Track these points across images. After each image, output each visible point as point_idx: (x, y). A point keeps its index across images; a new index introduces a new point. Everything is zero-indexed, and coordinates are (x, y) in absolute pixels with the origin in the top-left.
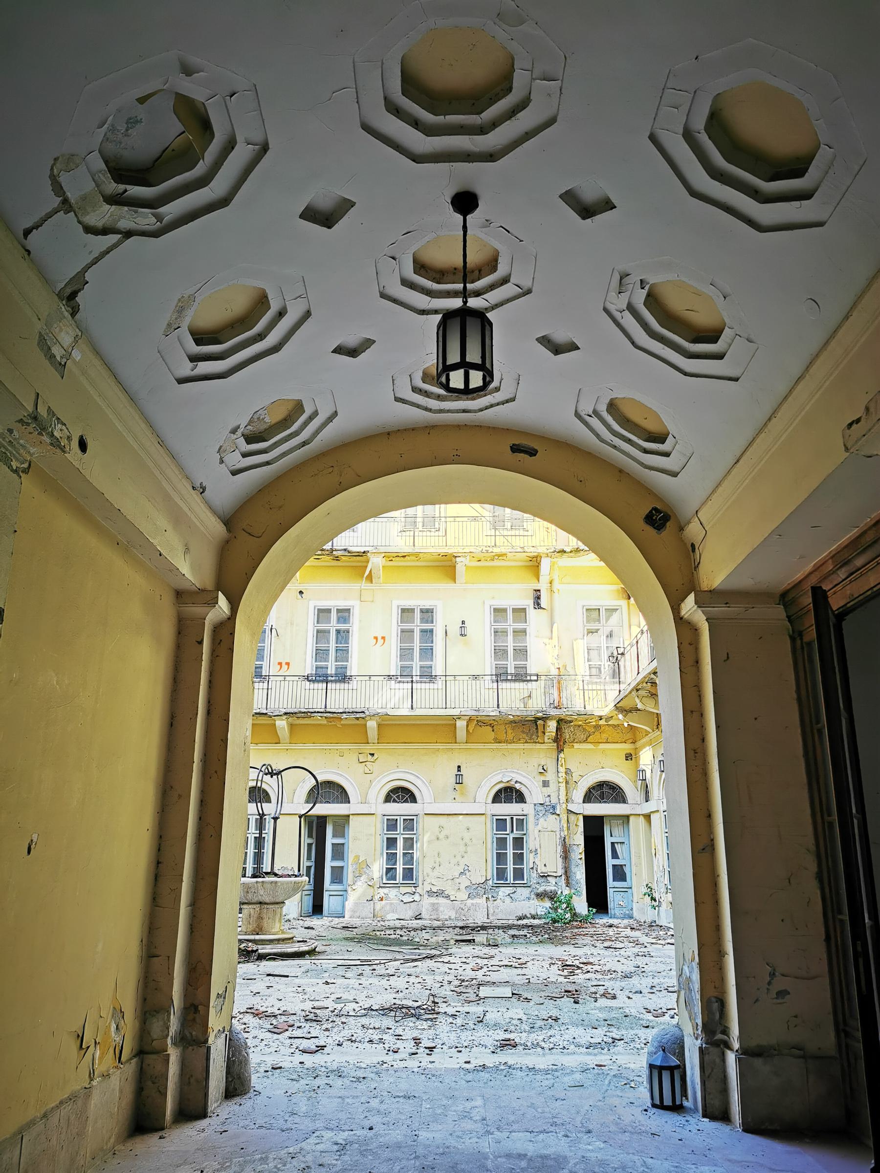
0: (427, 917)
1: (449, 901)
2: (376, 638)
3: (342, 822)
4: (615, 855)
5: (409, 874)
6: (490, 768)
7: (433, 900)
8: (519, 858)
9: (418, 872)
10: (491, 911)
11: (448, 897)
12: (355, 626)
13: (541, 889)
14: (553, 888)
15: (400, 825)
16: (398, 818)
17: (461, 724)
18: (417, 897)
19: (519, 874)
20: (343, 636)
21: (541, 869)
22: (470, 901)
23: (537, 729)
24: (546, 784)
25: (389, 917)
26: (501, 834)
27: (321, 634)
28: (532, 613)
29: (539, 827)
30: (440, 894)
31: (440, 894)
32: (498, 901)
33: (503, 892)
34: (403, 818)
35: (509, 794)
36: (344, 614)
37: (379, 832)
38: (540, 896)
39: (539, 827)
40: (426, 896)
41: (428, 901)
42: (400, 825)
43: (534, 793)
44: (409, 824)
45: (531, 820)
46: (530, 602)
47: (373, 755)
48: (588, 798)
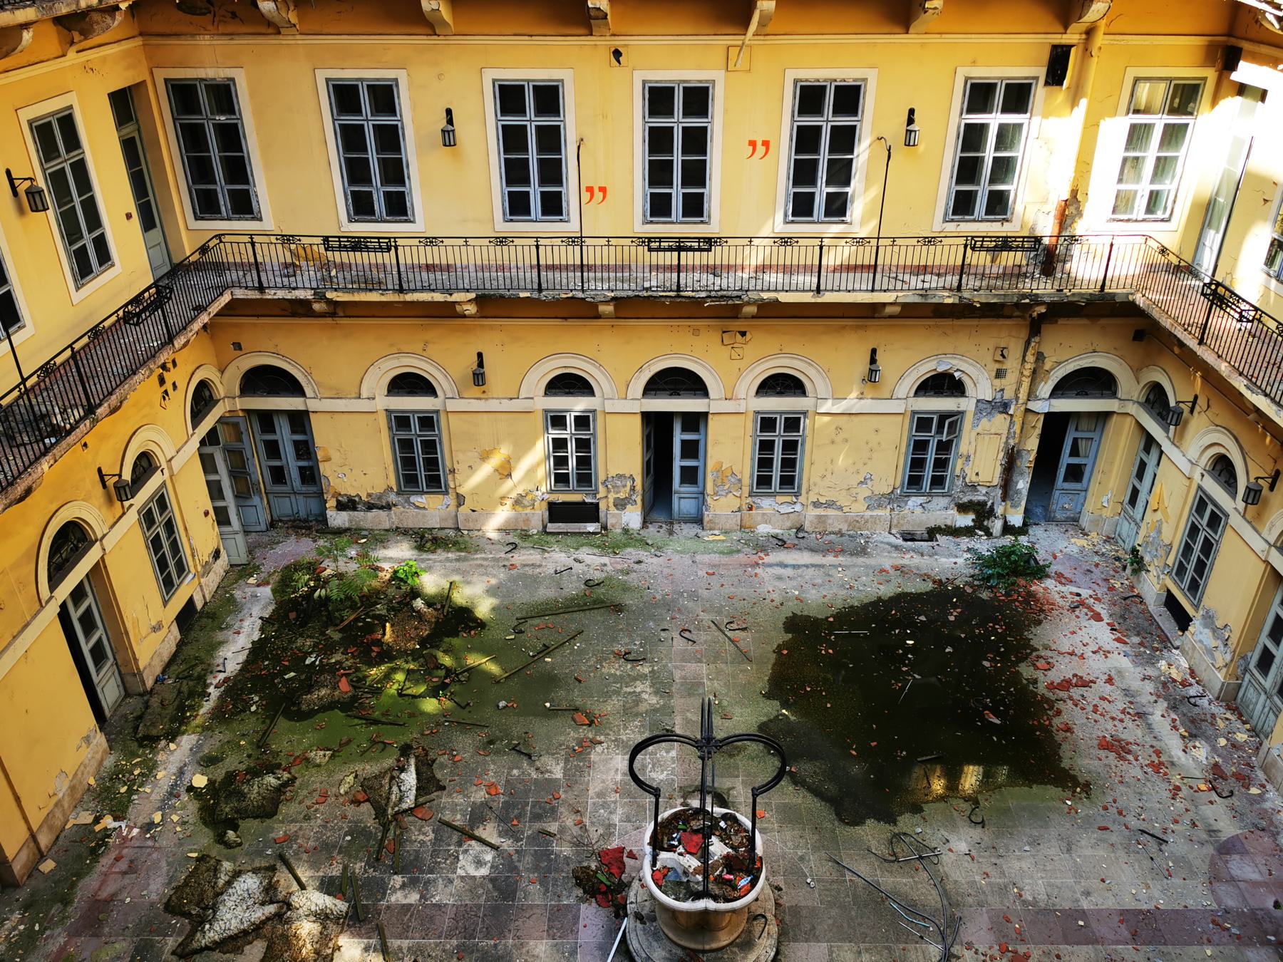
0: (810, 530)
2: (753, 144)
3: (695, 421)
4: (1075, 452)
7: (820, 512)
8: (941, 464)
9: (801, 479)
10: (895, 522)
11: (841, 508)
12: (719, 124)
13: (965, 500)
14: (982, 498)
18: (798, 508)
19: (938, 481)
20: (697, 141)
21: (971, 478)
22: (869, 513)
24: (1000, 374)
26: (922, 436)
29: (979, 429)
31: (830, 504)
33: (914, 502)
36: (698, 99)
37: (750, 431)
38: (963, 508)
39: (979, 429)
40: (811, 507)
41: (813, 512)
42: (780, 425)
43: (981, 386)
44: (793, 423)
46: (1042, 72)
48: (1061, 389)
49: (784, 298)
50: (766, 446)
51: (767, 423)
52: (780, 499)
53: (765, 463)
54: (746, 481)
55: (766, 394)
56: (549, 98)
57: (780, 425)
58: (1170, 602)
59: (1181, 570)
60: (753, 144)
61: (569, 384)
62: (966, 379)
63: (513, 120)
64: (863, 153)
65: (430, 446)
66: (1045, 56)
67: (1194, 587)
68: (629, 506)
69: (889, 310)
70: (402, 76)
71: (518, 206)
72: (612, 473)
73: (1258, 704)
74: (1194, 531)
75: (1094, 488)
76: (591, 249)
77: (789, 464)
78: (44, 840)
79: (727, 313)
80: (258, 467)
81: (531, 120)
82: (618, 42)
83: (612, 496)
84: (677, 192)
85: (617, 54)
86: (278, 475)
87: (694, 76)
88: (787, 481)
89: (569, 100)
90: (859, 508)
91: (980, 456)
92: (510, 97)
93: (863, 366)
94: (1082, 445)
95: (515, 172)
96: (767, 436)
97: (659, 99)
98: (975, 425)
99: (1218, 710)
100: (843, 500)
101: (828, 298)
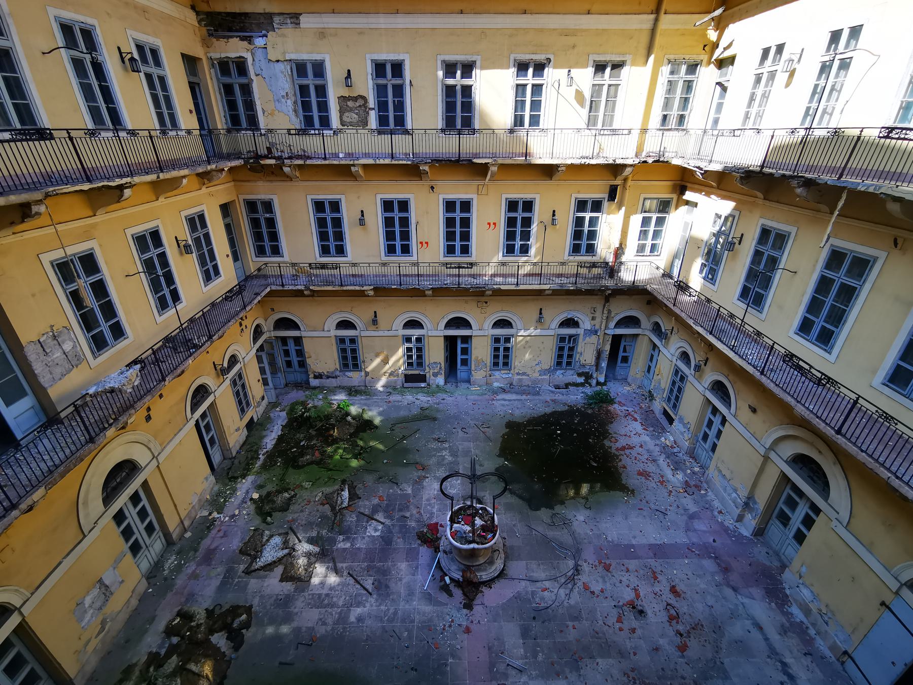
2: (489, 224)
3: (466, 339)
4: (625, 351)
7: (519, 377)
8: (570, 356)
12: (475, 216)
19: (569, 364)
20: (466, 223)
21: (583, 362)
24: (593, 319)
26: (562, 344)
30: (524, 374)
31: (524, 374)
33: (559, 372)
35: (570, 323)
36: (466, 206)
38: (579, 375)
42: (502, 341)
45: (581, 337)
46: (606, 196)
48: (619, 324)
49: (503, 287)
50: (497, 349)
51: (497, 340)
52: (503, 372)
53: (496, 357)
54: (488, 364)
56: (404, 205)
57: (502, 341)
58: (665, 413)
59: (669, 399)
60: (489, 224)
61: (413, 324)
62: (580, 321)
63: (389, 215)
64: (534, 228)
65: (354, 351)
66: (608, 190)
67: (675, 406)
69: (547, 292)
70: (343, 197)
71: (391, 250)
72: (432, 361)
73: (703, 455)
74: (674, 383)
75: (632, 366)
77: (506, 357)
78: (187, 523)
79: (480, 294)
80: (280, 361)
81: (397, 215)
82: (433, 183)
83: (432, 371)
84: (458, 244)
85: (432, 188)
86: (289, 364)
87: (464, 196)
88: (506, 364)
89: (412, 206)
90: (536, 375)
91: (586, 353)
92: (388, 205)
93: (537, 315)
94: (627, 348)
95: (390, 236)
96: (497, 345)
97: (450, 206)
98: (584, 340)
99: (686, 458)
100: (529, 372)
101: (522, 287)
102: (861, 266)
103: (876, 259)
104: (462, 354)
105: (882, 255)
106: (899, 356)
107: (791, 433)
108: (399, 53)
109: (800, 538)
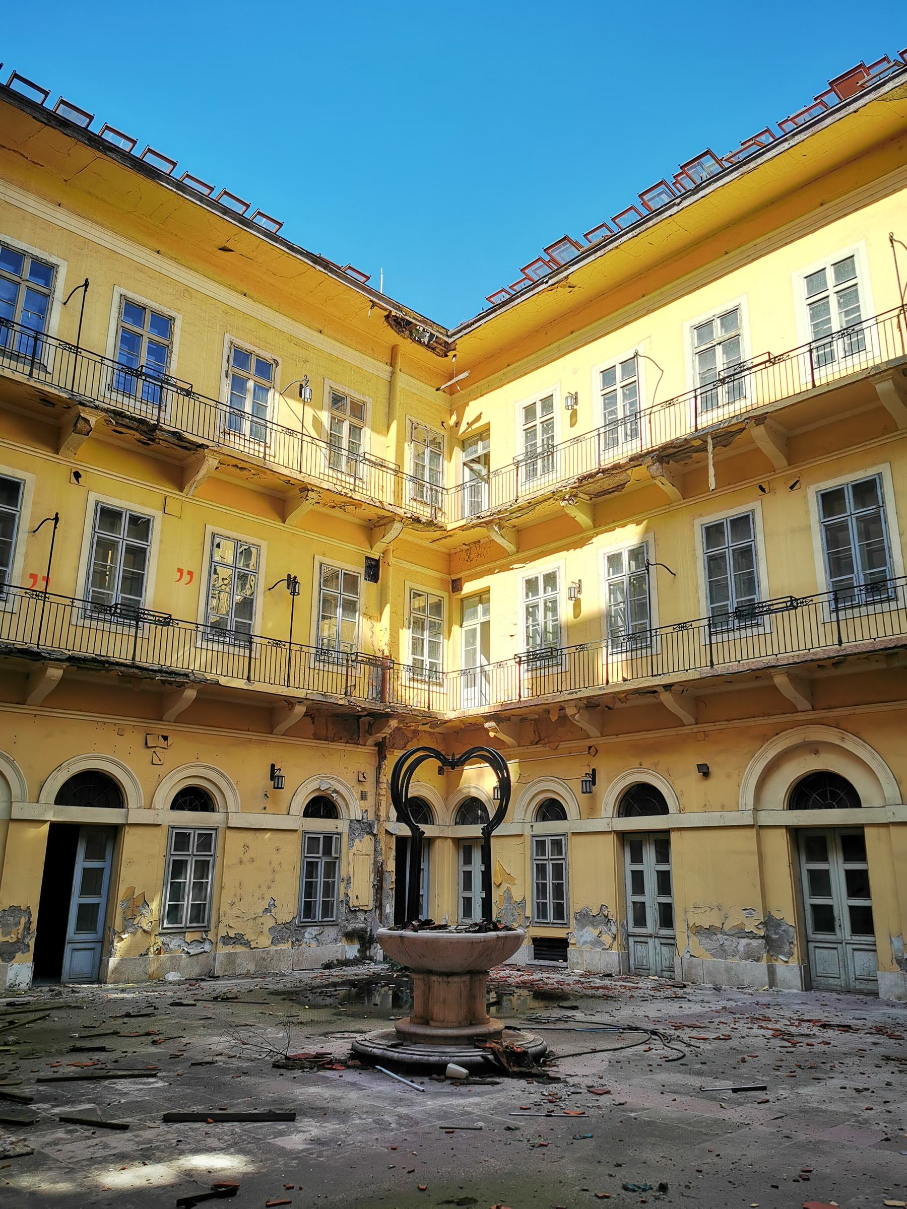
1: (247, 950)
2: (180, 571)
5: (198, 913)
6: (312, 769)
7: (229, 949)
8: (329, 889)
13: (350, 928)
14: (363, 925)
15: (194, 841)
16: (192, 831)
17: (300, 710)
18: (207, 947)
19: (327, 908)
20: (138, 556)
21: (353, 902)
22: (273, 948)
23: (358, 727)
24: (363, 796)
25: (172, 976)
27: (103, 547)
28: (363, 584)
30: (238, 940)
31: (238, 940)
32: (304, 945)
34: (198, 832)
38: (350, 936)
39: (354, 850)
40: (220, 945)
41: (223, 950)
42: (194, 841)
44: (206, 840)
45: (345, 838)
46: (362, 570)
47: (165, 738)
55: (181, 808)
60: (180, 571)
62: (340, 801)
68: (18, 955)
73: (651, 953)
76: (54, 606)
85: (77, 475)
102: (742, 524)
103: (753, 511)
104: (84, 892)
105: (756, 505)
106: (828, 575)
107: (771, 754)
108: (51, 254)
109: (863, 921)
